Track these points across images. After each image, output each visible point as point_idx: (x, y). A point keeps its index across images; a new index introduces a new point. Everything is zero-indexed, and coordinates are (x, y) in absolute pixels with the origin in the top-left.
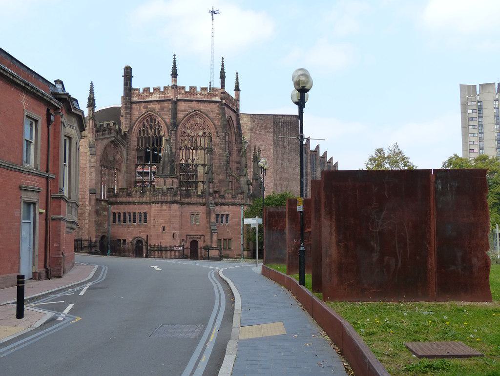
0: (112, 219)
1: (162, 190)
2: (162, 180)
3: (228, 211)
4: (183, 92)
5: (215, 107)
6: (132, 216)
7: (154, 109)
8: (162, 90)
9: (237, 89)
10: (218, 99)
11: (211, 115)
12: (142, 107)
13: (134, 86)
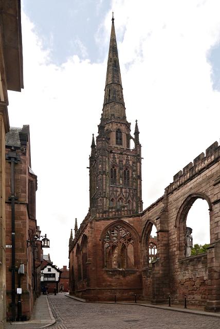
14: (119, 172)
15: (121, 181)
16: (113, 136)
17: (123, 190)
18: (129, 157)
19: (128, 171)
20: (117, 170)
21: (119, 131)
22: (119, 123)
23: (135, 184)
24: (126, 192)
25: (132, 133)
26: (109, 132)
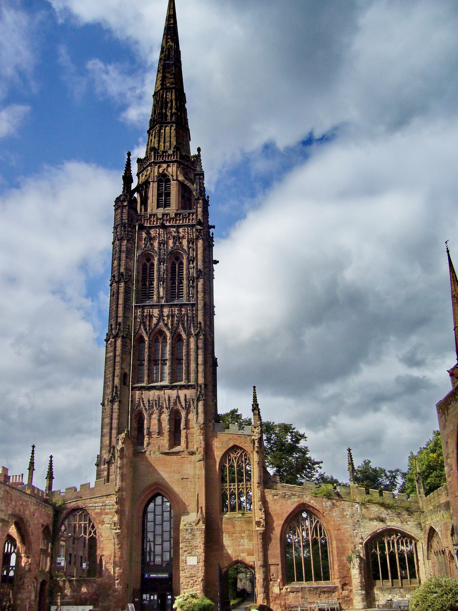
15: (161, 289)
17: (166, 311)
18: (181, 230)
22: (165, 162)
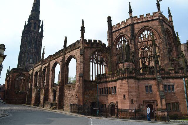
0: (99, 92)
1: (122, 71)
2: (122, 64)
3: (173, 82)
4: (136, 19)
5: (156, 23)
6: (109, 90)
7: (123, 32)
8: (125, 22)
9: (170, 15)
10: (157, 18)
11: (155, 27)
12: (117, 33)
13: (113, 25)
14: (33, 42)
16: (33, 25)
17: (34, 50)
19: (37, 42)
20: (32, 40)
21: (35, 23)
23: (39, 47)
24: (35, 51)
25: (41, 24)
26: (31, 23)
